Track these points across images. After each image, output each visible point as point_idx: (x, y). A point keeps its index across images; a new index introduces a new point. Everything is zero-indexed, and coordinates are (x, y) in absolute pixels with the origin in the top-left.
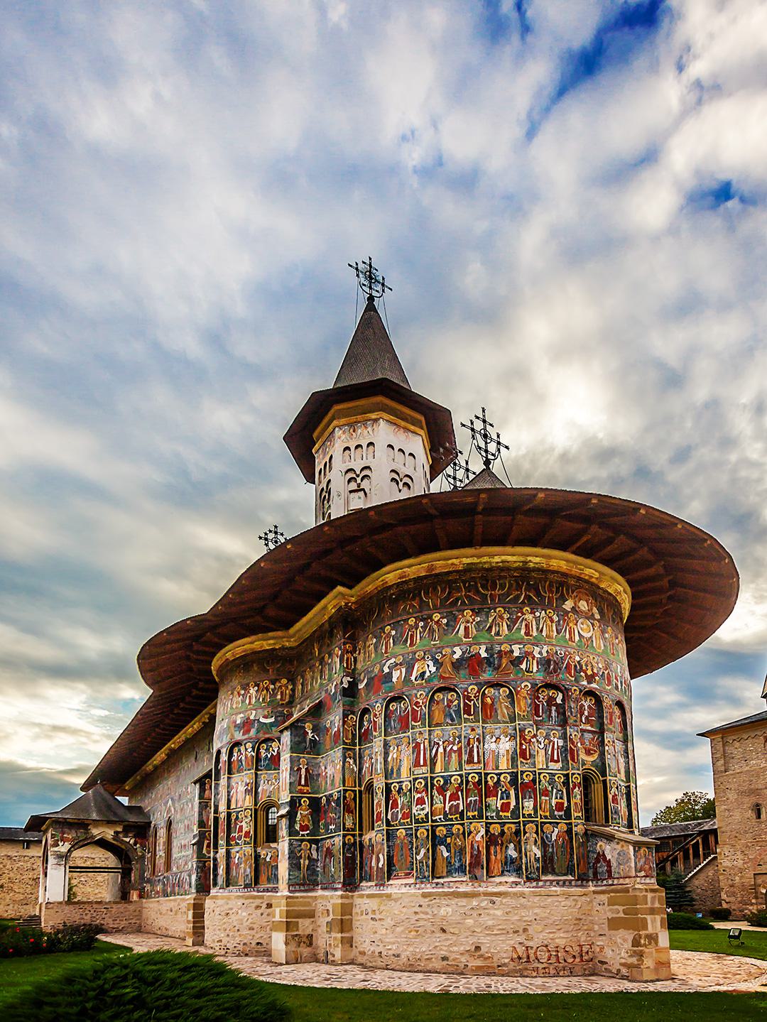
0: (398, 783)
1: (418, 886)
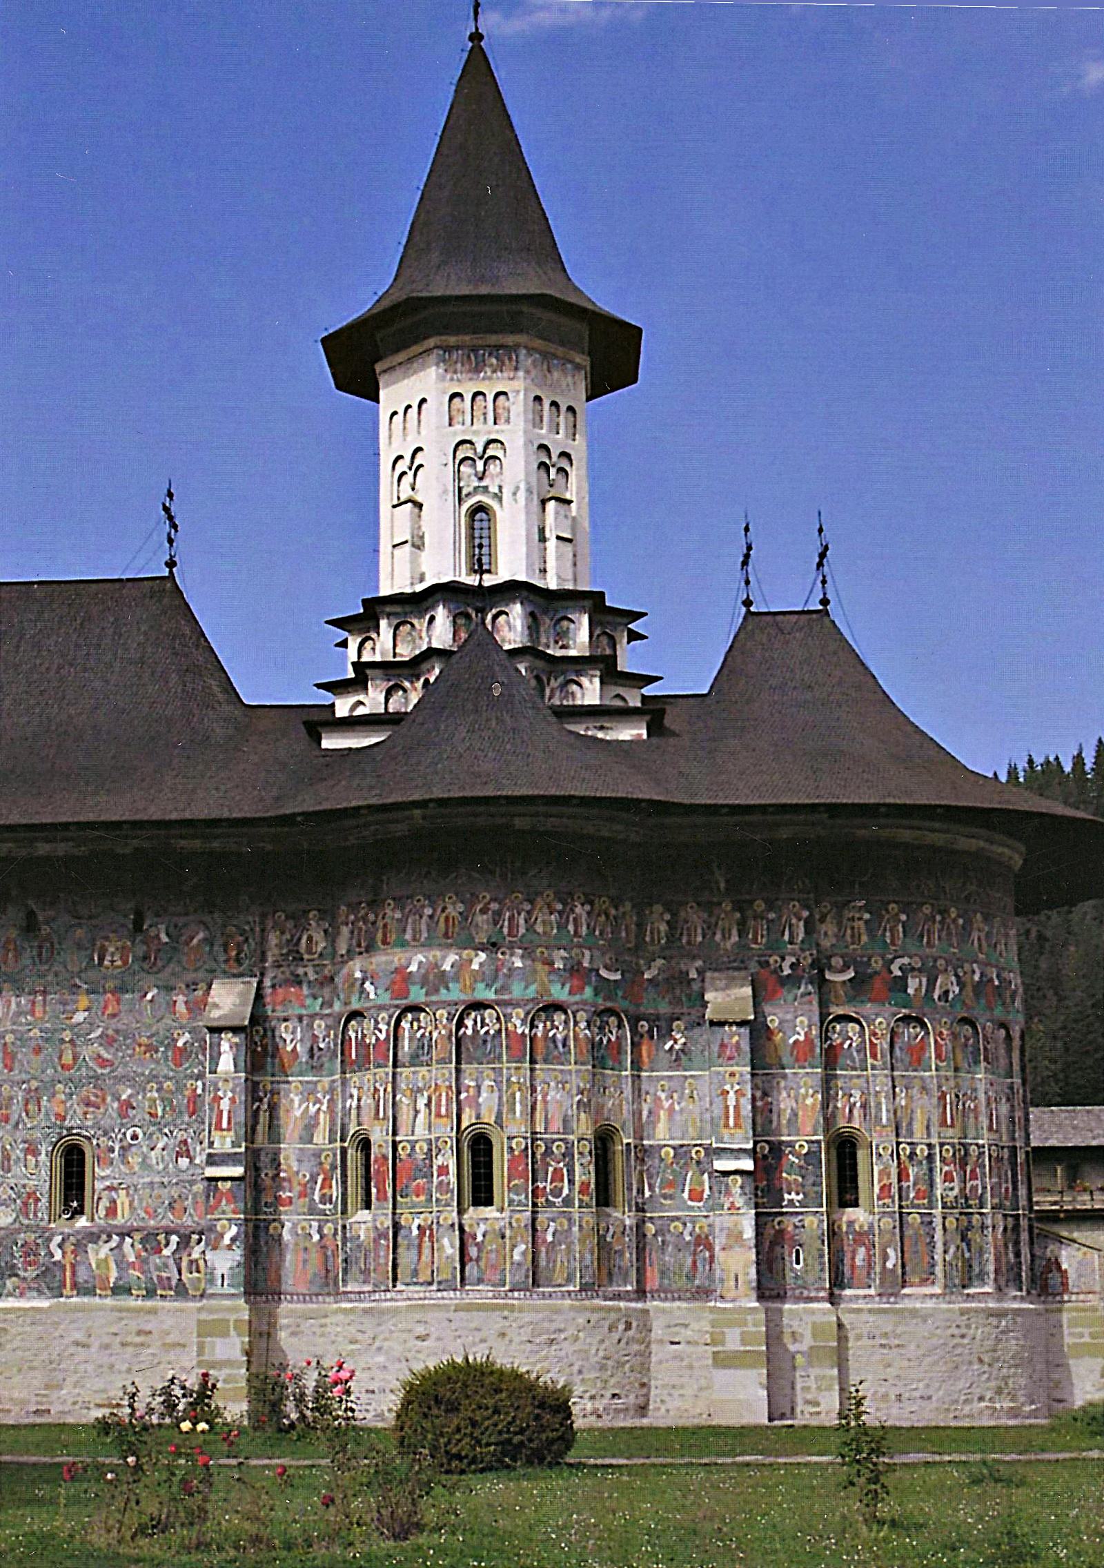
0: (908, 1144)
1: (947, 1298)
